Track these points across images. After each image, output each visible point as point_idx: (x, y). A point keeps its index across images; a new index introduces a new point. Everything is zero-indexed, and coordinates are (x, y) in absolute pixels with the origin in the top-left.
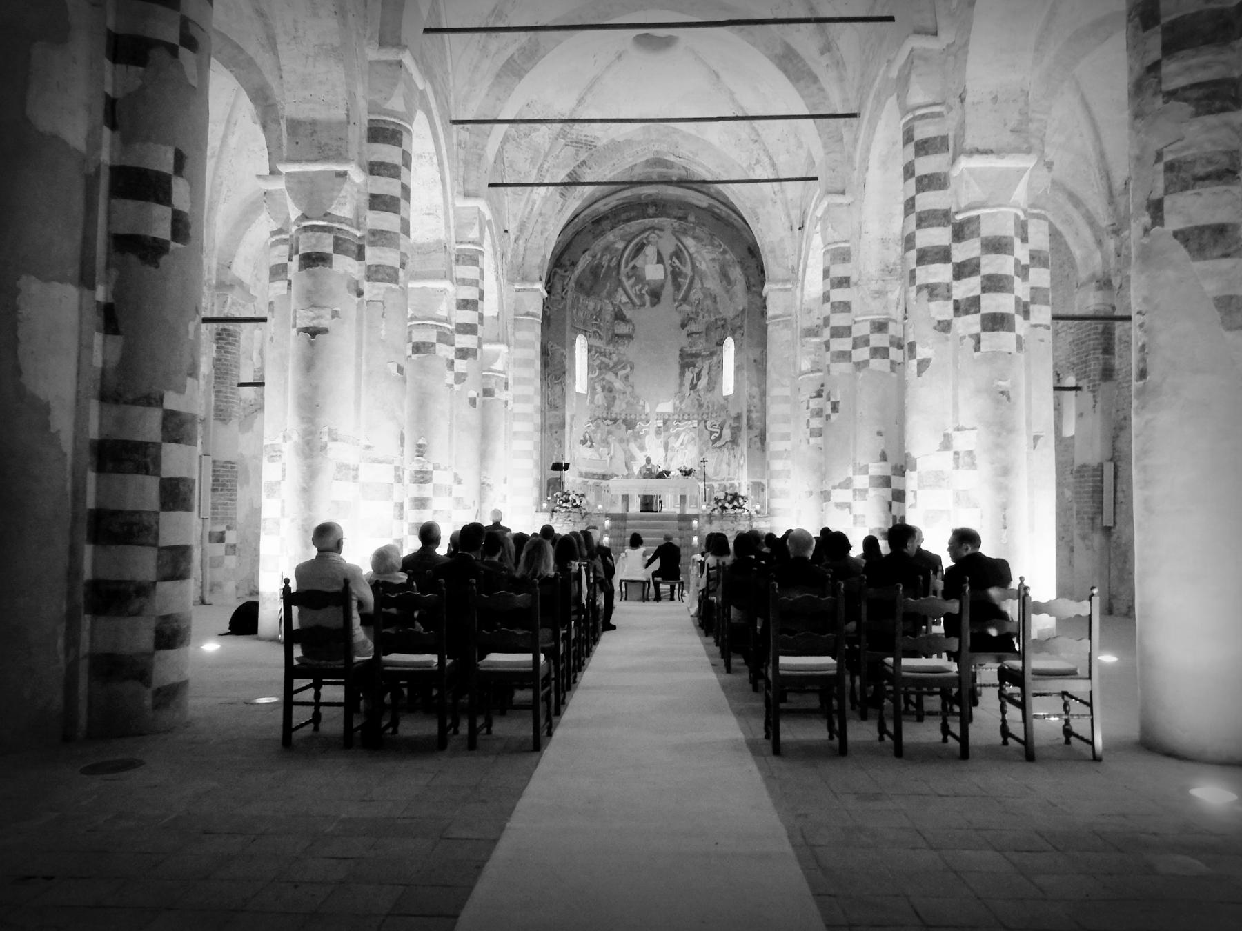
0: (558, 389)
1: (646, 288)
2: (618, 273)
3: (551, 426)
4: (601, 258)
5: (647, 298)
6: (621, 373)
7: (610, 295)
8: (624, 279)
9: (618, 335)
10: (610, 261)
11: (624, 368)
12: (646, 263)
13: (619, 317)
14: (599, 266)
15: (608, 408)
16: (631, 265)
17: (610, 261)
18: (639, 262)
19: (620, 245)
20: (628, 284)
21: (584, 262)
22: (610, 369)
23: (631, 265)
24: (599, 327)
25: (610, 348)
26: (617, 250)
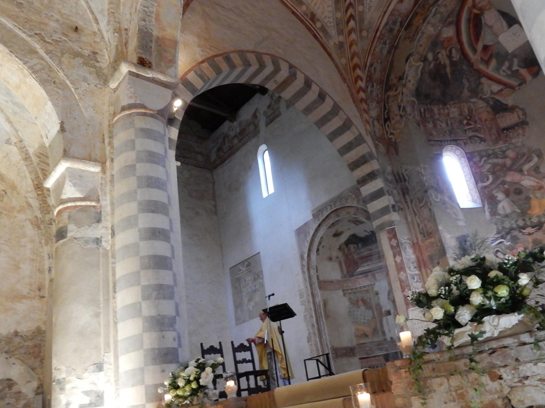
0: (425, 213)
1: (516, 61)
2: (471, 65)
3: (431, 258)
4: (436, 59)
5: (524, 72)
6: (526, 167)
7: (475, 92)
8: (482, 67)
9: (504, 129)
10: (450, 56)
11: (529, 160)
12: (497, 35)
13: (499, 108)
14: (439, 67)
15: (524, 214)
16: (480, 47)
17: (450, 56)
18: (487, 38)
19: (449, 32)
20: (490, 70)
21: (412, 72)
22: (510, 169)
23: (480, 47)
24: (476, 130)
25: (501, 145)
26: (449, 39)
